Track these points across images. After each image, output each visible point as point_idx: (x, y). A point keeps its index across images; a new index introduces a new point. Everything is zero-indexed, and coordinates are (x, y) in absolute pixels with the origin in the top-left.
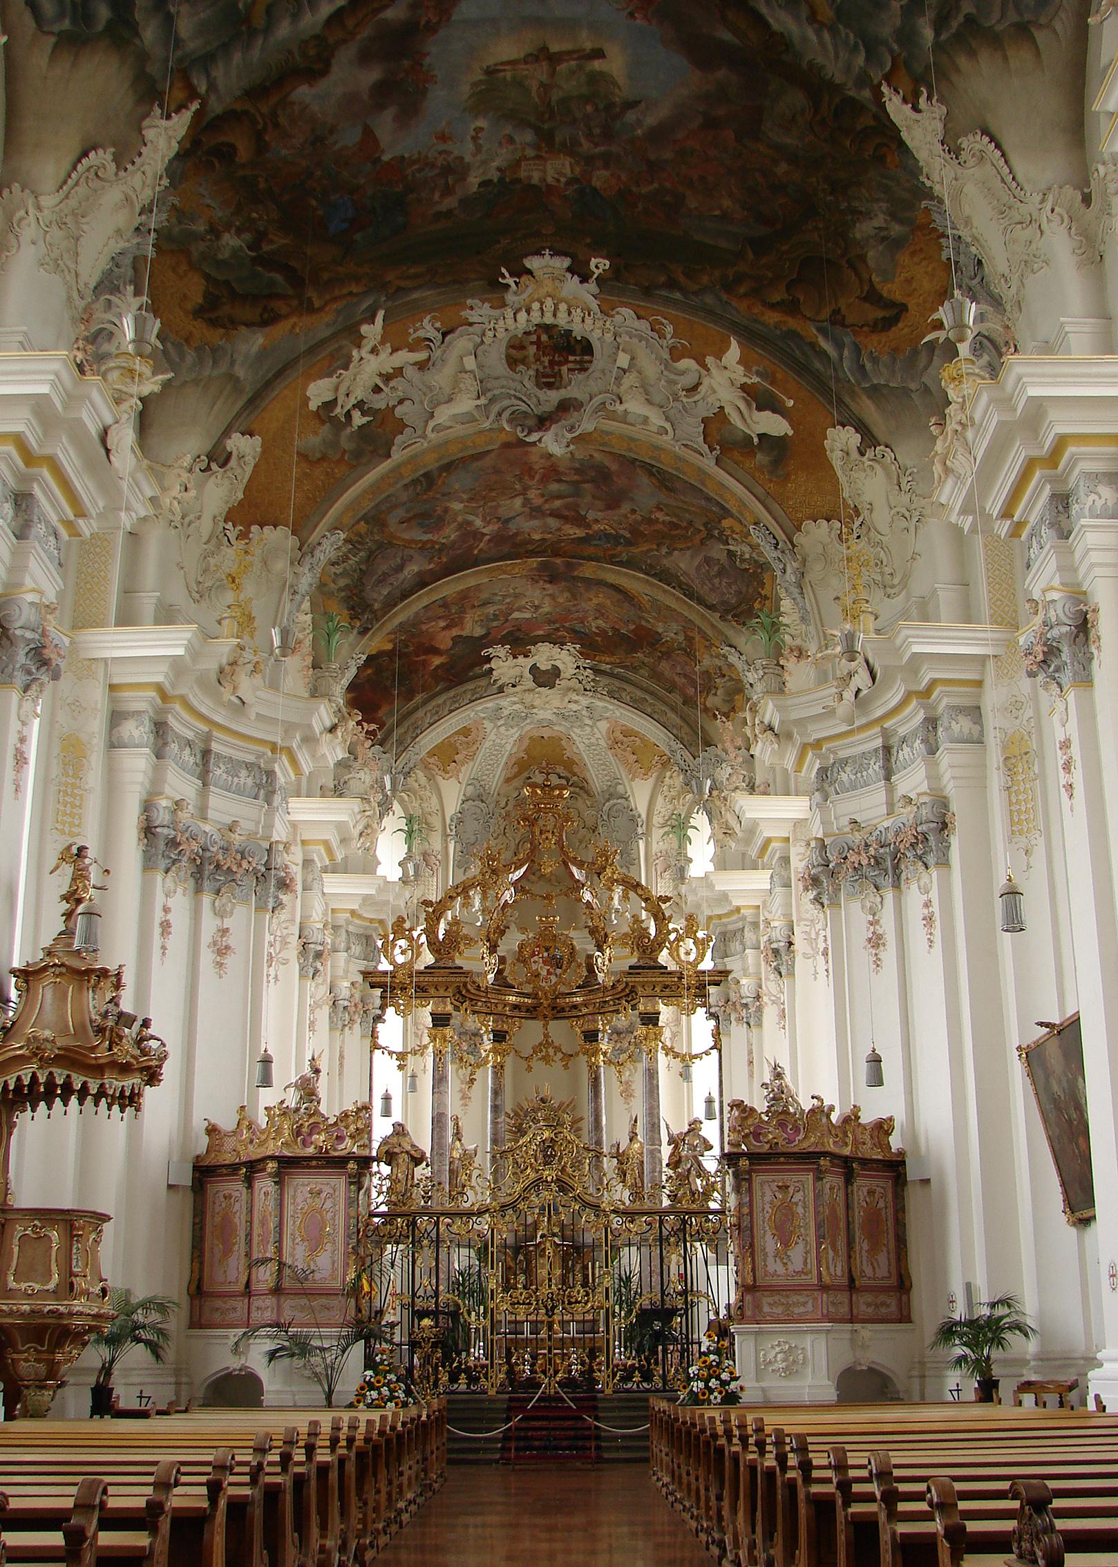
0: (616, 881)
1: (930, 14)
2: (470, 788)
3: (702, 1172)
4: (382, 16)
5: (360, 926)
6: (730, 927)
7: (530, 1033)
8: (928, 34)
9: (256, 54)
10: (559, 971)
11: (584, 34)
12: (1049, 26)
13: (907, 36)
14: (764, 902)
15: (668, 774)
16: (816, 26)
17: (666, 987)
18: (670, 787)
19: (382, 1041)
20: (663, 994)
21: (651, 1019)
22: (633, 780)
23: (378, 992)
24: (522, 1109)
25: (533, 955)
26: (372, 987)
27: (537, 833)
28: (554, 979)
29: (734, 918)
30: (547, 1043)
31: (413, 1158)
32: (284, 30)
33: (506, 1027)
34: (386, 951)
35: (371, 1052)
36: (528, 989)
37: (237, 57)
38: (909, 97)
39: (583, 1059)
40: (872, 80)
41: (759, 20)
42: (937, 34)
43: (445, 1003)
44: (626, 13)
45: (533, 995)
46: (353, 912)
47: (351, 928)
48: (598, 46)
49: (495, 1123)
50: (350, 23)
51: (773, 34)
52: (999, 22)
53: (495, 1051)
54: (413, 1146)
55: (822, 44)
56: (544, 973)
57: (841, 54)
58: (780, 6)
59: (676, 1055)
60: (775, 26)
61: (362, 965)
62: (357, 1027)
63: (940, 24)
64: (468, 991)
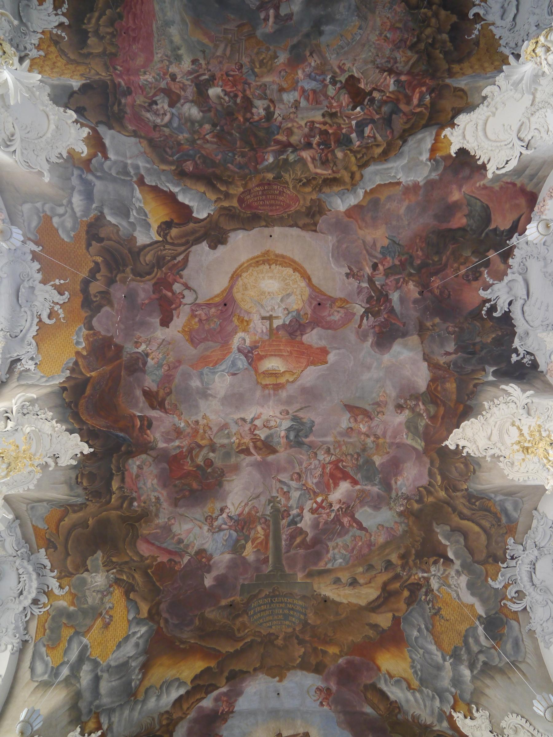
1: (466, 663)
4: (201, 704)
8: (467, 673)
9: (136, 714)
11: (299, 722)
12: (524, 661)
13: (457, 681)
16: (412, 691)
32: (152, 703)
37: (126, 712)
38: (467, 713)
40: (445, 713)
41: (383, 695)
42: (472, 672)
44: (318, 702)
48: (306, 731)
50: (185, 707)
51: (392, 703)
52: (500, 662)
55: (416, 700)
57: (427, 704)
58: (392, 685)
60: (392, 697)
63: (472, 667)
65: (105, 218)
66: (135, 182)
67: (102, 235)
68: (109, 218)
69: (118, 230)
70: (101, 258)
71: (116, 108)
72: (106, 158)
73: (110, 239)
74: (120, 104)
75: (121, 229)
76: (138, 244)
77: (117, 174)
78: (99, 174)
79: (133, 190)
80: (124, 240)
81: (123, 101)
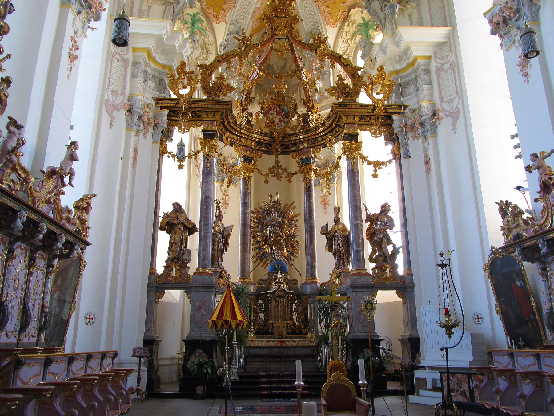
0: (327, 55)
2: (232, 26)
3: (389, 242)
5: (155, 70)
6: (404, 80)
7: (267, 161)
10: (286, 120)
14: (435, 53)
15: (347, 24)
17: (362, 117)
18: (347, 33)
19: (169, 149)
20: (360, 123)
21: (353, 138)
22: (327, 24)
23: (166, 112)
24: (261, 208)
25: (270, 109)
26: (162, 108)
27: (275, 27)
28: (283, 125)
29: (410, 70)
30: (277, 166)
31: (187, 228)
33: (252, 155)
34: (173, 86)
35: (160, 155)
36: (266, 130)
39: (301, 176)
43: (213, 124)
45: (270, 135)
46: (149, 52)
47: (148, 70)
49: (244, 214)
53: (245, 168)
54: (187, 220)
56: (277, 120)
59: (369, 163)
61: (157, 94)
62: (149, 135)
64: (229, 123)
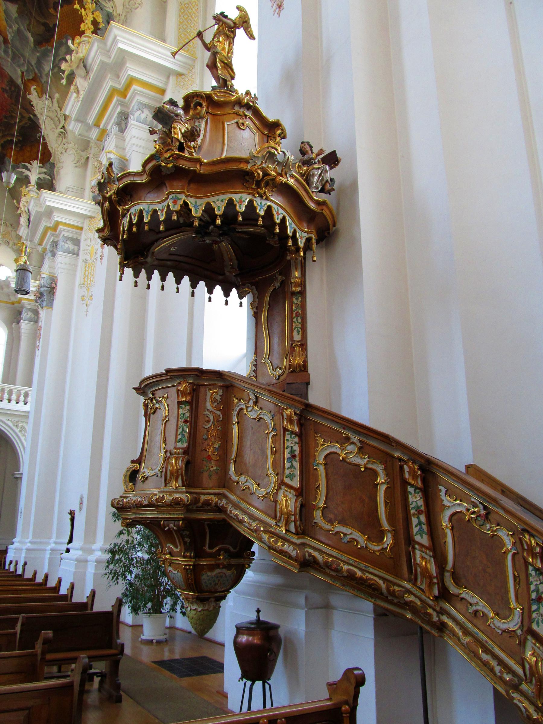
65: (34, 40)
66: (9, 43)
67: (42, 28)
68: (32, 39)
69: (29, 25)
70: (50, 11)
71: (13, 89)
72: (23, 73)
73: (38, 21)
74: (10, 89)
75: (26, 25)
76: (17, 6)
77: (19, 58)
78: (31, 68)
79: (12, 40)
80: (27, 15)
81: (8, 88)
